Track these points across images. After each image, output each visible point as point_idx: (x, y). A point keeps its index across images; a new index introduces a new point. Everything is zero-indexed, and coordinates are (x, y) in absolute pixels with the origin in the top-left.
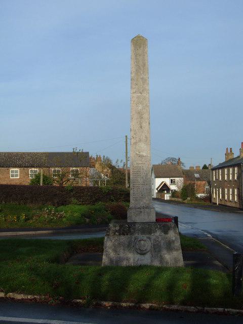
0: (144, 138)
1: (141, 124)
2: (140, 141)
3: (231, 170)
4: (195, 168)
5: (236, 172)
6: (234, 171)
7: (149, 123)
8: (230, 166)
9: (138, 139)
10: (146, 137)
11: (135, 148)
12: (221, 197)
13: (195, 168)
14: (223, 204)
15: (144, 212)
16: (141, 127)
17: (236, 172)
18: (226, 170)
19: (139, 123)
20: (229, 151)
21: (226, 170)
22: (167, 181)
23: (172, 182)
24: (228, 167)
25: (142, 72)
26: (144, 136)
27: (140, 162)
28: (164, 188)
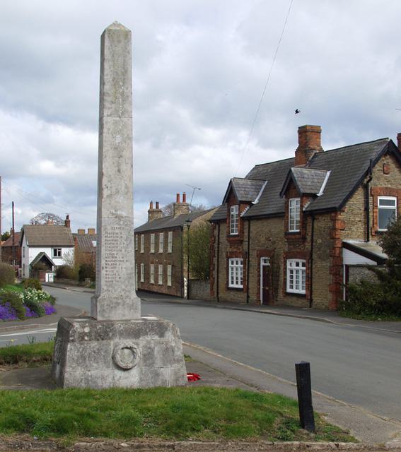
0: (123, 188)
1: (119, 165)
2: (117, 192)
3: (161, 235)
4: (86, 232)
5: (170, 239)
6: (166, 237)
7: (132, 166)
8: (161, 230)
9: (114, 189)
10: (127, 187)
11: (110, 204)
12: (142, 280)
13: (86, 232)
14: (146, 289)
15: (123, 305)
16: (119, 171)
17: (170, 239)
18: (153, 236)
19: (116, 164)
20: (154, 207)
21: (153, 236)
22: (49, 252)
23: (55, 255)
24: (156, 232)
25: (121, 84)
26: (124, 185)
27: (116, 226)
28: (44, 262)
